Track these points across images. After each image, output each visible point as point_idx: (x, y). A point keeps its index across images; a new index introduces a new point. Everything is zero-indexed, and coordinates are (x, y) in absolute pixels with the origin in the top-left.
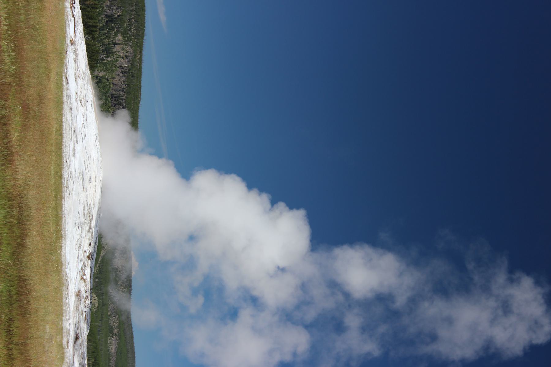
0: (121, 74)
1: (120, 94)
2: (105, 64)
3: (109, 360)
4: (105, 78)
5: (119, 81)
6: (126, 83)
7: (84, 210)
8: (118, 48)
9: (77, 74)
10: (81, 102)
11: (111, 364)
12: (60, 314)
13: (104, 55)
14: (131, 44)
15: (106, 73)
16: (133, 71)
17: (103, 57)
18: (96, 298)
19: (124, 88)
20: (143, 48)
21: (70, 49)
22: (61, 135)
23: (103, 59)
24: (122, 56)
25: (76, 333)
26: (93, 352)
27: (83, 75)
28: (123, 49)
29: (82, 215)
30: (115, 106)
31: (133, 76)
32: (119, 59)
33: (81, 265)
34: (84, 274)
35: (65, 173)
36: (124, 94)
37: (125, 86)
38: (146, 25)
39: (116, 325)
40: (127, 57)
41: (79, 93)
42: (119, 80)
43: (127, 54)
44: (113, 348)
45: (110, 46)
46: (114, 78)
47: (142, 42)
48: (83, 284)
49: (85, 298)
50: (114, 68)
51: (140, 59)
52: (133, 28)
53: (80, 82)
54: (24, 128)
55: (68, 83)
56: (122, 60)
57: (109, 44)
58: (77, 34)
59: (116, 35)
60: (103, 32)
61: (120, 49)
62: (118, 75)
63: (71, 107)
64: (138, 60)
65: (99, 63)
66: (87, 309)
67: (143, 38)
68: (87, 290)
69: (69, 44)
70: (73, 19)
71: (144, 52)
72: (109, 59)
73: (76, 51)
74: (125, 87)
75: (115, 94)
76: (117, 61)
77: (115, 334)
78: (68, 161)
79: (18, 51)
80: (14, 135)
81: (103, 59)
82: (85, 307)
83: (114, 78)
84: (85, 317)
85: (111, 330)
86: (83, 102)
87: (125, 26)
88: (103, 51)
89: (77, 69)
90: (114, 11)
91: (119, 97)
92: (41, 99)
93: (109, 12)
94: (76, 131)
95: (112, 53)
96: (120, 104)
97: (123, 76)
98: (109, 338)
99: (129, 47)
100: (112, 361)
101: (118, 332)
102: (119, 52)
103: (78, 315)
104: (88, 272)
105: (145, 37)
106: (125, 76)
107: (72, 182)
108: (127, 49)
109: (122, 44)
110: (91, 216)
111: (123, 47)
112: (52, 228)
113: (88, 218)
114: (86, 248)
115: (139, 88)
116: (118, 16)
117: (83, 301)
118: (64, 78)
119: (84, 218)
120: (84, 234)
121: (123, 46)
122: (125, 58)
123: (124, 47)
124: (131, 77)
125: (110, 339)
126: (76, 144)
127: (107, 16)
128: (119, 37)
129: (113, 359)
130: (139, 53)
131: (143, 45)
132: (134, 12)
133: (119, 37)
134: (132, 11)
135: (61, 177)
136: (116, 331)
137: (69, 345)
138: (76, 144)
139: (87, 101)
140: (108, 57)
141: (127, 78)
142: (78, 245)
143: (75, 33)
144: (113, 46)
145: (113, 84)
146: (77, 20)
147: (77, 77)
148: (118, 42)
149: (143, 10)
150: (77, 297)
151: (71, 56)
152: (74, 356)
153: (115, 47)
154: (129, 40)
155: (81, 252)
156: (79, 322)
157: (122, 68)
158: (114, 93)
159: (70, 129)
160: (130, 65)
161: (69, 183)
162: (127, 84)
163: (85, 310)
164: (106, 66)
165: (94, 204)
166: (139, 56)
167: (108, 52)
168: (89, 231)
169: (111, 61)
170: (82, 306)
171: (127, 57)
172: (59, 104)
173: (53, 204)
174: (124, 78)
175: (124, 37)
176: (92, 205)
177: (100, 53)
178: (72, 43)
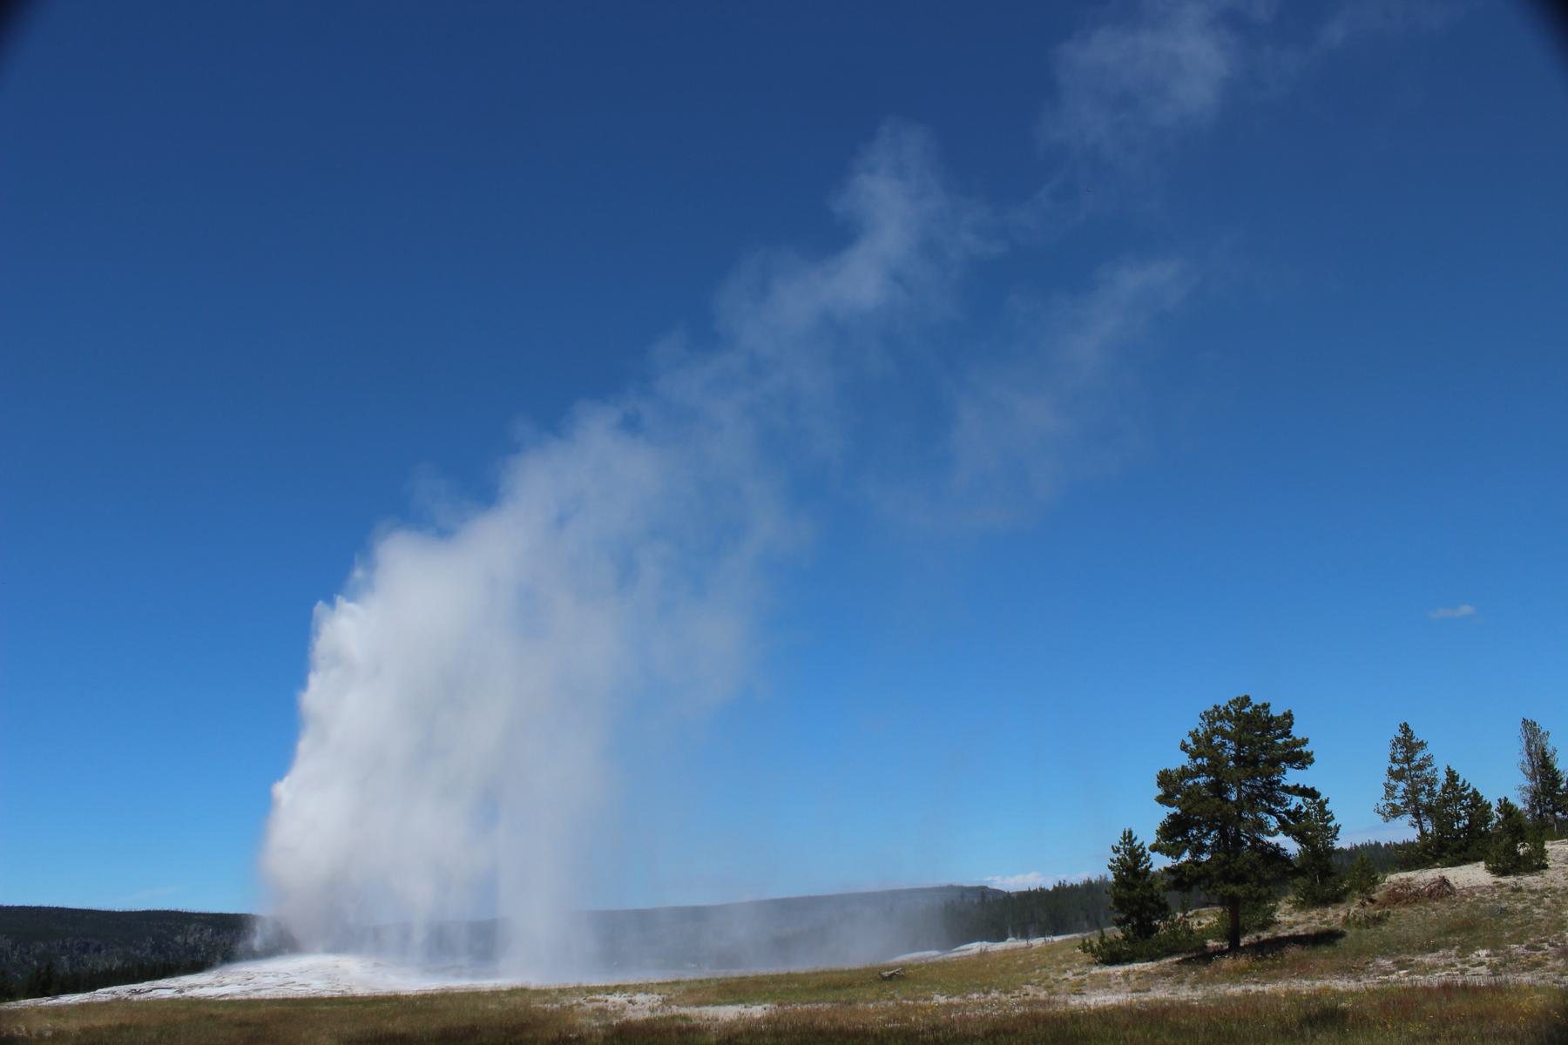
0: (221, 936)
2: (208, 954)
8: (191, 940)
9: (216, 984)
12: (476, 995)
21: (188, 993)
22: (285, 1001)
28: (191, 935)
35: (327, 994)
38: (166, 908)
40: (201, 930)
41: (239, 982)
43: (198, 929)
46: (224, 944)
53: (227, 980)
55: (227, 995)
56: (205, 934)
58: (172, 985)
59: (175, 943)
60: (171, 958)
61: (192, 939)
62: (221, 939)
63: (254, 990)
70: (154, 992)
71: (196, 912)
72: (203, 949)
73: (191, 987)
87: (165, 932)
89: (211, 985)
90: (148, 945)
92: (242, 1024)
93: (148, 951)
102: (195, 939)
105: (180, 910)
112: (386, 1005)
116: (153, 940)
118: (222, 999)
121: (188, 936)
127: (153, 953)
128: (178, 938)
132: (151, 923)
133: (178, 938)
140: (200, 951)
143: (170, 988)
148: (183, 940)
151: (197, 992)
161: (338, 990)
167: (194, 950)
171: (201, 930)
173: (360, 1006)
178: (181, 991)
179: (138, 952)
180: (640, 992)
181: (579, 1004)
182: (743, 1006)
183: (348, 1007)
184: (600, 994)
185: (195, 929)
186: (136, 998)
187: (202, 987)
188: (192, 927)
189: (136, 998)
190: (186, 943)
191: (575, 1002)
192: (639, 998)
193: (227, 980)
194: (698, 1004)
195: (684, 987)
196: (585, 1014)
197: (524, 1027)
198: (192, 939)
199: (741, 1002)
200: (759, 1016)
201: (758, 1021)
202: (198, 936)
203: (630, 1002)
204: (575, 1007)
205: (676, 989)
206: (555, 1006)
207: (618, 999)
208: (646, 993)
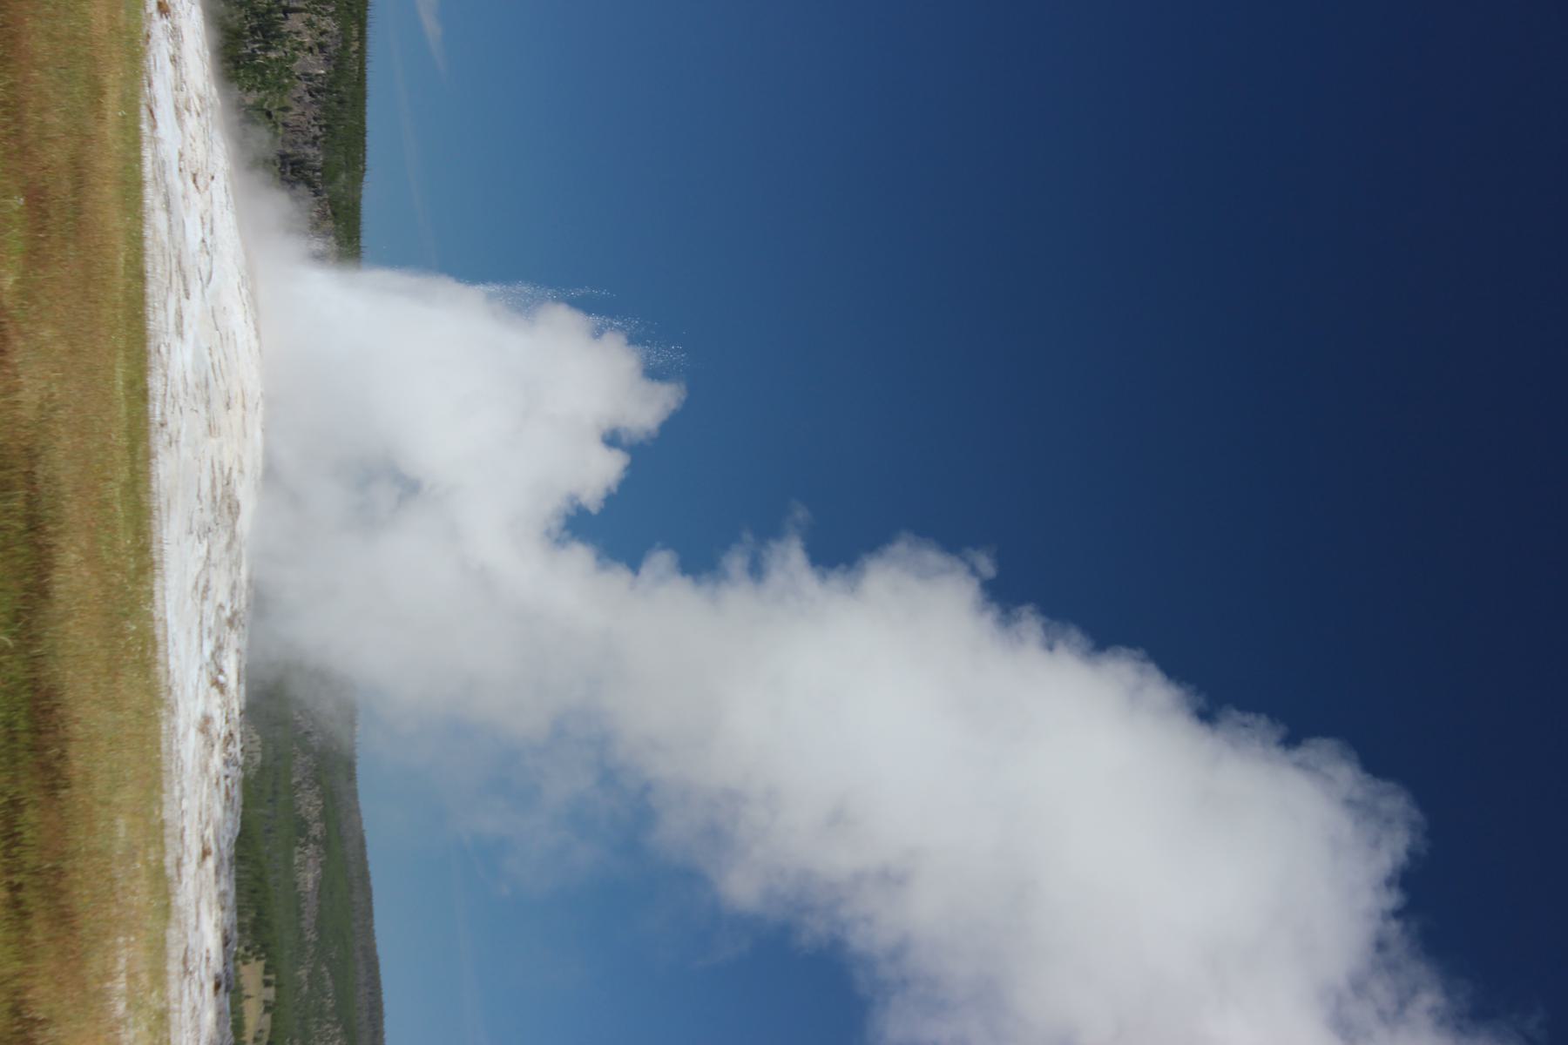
0: (307, 98)
1: (307, 155)
2: (260, 69)
3: (300, 912)
4: (265, 110)
5: (302, 119)
6: (323, 122)
7: (213, 486)
8: (295, 22)
10: (195, 181)
11: (304, 924)
13: (255, 42)
14: (331, 9)
15: (263, 92)
16: (343, 88)
17: (253, 50)
18: (257, 737)
19: (316, 138)
20: (369, 20)
21: (158, 27)
22: (141, 277)
23: (253, 56)
24: (307, 45)
25: (202, 837)
26: (254, 891)
27: (197, 102)
28: (310, 24)
29: (207, 502)
31: (341, 102)
32: (300, 54)
33: (208, 647)
34: (221, 671)
35: (156, 383)
36: (317, 153)
37: (321, 130)
39: (316, 813)
40: (322, 47)
41: (188, 154)
42: (301, 111)
43: (323, 39)
44: (308, 878)
45: (274, 16)
46: (286, 109)
48: (217, 699)
49: (226, 738)
50: (286, 81)
51: (361, 51)
53: (192, 123)
55: (154, 127)
56: (309, 57)
57: (270, 11)
61: (300, 26)
62: (299, 100)
64: (355, 56)
65: (242, 67)
66: (231, 768)
68: (230, 716)
69: (156, 16)
72: (272, 55)
73: (175, 34)
74: (319, 133)
75: (293, 155)
76: (294, 59)
77: (315, 837)
78: (163, 349)
81: (253, 56)
82: (226, 763)
84: (227, 794)
85: (302, 827)
86: (200, 181)
88: (253, 31)
89: (178, 87)
92: (79, 172)
94: (183, 265)
95: (279, 36)
97: (312, 103)
98: (297, 849)
99: (329, 20)
100: (305, 916)
101: (321, 833)
102: (298, 33)
103: (205, 785)
104: (231, 665)
106: (317, 102)
107: (177, 408)
109: (306, 11)
110: (234, 505)
111: (309, 20)
112: (125, 540)
113: (226, 511)
114: (221, 595)
117: (218, 747)
119: (213, 510)
120: (215, 556)
121: (305, 15)
122: (316, 50)
123: (314, 18)
124: (335, 104)
125: (300, 853)
126: (184, 300)
129: (310, 909)
130: (355, 33)
131: (369, 13)
136: (316, 830)
137: (183, 870)
138: (184, 300)
139: (213, 178)
140: (268, 48)
141: (325, 109)
142: (200, 588)
144: (282, 15)
145: (285, 125)
147: (181, 106)
150: (200, 736)
151: (160, 50)
152: (198, 902)
153: (287, 18)
155: (209, 608)
156: (209, 809)
157: (310, 80)
159: (167, 258)
160: (332, 69)
161: (168, 413)
162: (326, 126)
163: (227, 772)
164: (263, 75)
165: (241, 471)
166: (357, 44)
168: (229, 546)
169: (277, 60)
170: (216, 761)
171: (322, 47)
172: (132, 187)
173: (124, 475)
174: (315, 110)
176: (235, 474)
177: (246, 37)
185: (323, 33)
187: (174, 60)
188: (328, 24)
193: (192, 123)
197: (64, 919)
198: (300, 26)
206: (121, 1007)
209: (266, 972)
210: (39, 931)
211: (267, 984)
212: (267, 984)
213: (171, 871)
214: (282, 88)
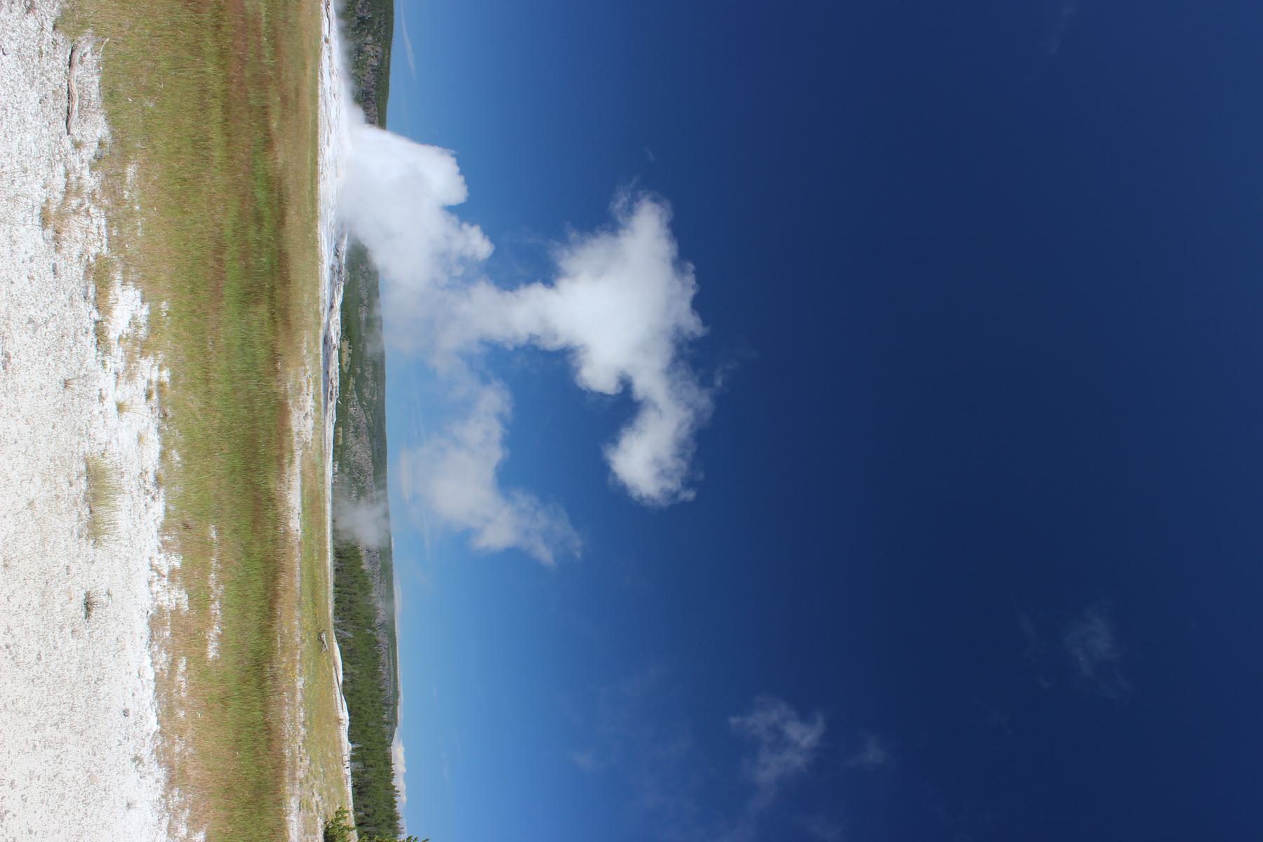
0: (371, 72)
8: (368, 48)
12: (316, 284)
21: (325, 47)
22: (316, 125)
28: (373, 49)
30: (365, 101)
31: (382, 74)
32: (370, 58)
34: (338, 251)
35: (320, 160)
38: (394, 28)
43: (377, 54)
46: (364, 76)
47: (391, 43)
51: (389, 58)
52: (382, 30)
53: (334, 78)
54: (283, 118)
55: (322, 78)
56: (372, 59)
58: (332, 34)
59: (367, 35)
61: (370, 49)
62: (369, 73)
67: (391, 39)
69: (324, 43)
70: (327, 19)
72: (361, 58)
73: (330, 49)
79: (277, 48)
80: (274, 124)
83: (364, 76)
91: (368, 93)
92: (298, 92)
93: (361, 14)
96: (370, 99)
105: (393, 39)
108: (377, 49)
115: (388, 84)
116: (369, 18)
117: (336, 275)
118: (319, 73)
123: (374, 47)
128: (370, 38)
130: (387, 52)
133: (370, 38)
134: (382, 14)
135: (316, 163)
136: (366, 302)
140: (359, 56)
141: (377, 76)
145: (364, 81)
146: (331, 19)
148: (368, 42)
149: (392, 13)
151: (325, 53)
154: (379, 41)
158: (365, 89)
166: (387, 56)
171: (376, 56)
172: (315, 97)
173: (309, 188)
175: (374, 38)
178: (327, 41)
179: (360, 6)
180: (315, 423)
181: (305, 371)
182: (300, 511)
183: (309, 178)
184: (314, 389)
185: (377, 52)
186: (323, 6)
187: (329, 57)
188: (379, 49)
189: (323, 6)
190: (366, 44)
191: (308, 367)
192: (310, 423)
194: (303, 473)
195: (317, 460)
196: (297, 376)
197: (287, 323)
198: (370, 49)
199: (304, 509)
200: (291, 525)
201: (286, 525)
202: (372, 54)
203: (306, 414)
204: (303, 368)
205: (317, 454)
207: (309, 404)
208: (313, 429)
209: (349, 345)
210: (280, 327)
211: (350, 348)
212: (350, 348)
213: (321, 312)
214: (363, 69)
